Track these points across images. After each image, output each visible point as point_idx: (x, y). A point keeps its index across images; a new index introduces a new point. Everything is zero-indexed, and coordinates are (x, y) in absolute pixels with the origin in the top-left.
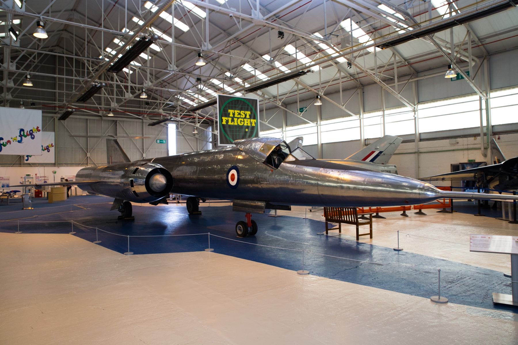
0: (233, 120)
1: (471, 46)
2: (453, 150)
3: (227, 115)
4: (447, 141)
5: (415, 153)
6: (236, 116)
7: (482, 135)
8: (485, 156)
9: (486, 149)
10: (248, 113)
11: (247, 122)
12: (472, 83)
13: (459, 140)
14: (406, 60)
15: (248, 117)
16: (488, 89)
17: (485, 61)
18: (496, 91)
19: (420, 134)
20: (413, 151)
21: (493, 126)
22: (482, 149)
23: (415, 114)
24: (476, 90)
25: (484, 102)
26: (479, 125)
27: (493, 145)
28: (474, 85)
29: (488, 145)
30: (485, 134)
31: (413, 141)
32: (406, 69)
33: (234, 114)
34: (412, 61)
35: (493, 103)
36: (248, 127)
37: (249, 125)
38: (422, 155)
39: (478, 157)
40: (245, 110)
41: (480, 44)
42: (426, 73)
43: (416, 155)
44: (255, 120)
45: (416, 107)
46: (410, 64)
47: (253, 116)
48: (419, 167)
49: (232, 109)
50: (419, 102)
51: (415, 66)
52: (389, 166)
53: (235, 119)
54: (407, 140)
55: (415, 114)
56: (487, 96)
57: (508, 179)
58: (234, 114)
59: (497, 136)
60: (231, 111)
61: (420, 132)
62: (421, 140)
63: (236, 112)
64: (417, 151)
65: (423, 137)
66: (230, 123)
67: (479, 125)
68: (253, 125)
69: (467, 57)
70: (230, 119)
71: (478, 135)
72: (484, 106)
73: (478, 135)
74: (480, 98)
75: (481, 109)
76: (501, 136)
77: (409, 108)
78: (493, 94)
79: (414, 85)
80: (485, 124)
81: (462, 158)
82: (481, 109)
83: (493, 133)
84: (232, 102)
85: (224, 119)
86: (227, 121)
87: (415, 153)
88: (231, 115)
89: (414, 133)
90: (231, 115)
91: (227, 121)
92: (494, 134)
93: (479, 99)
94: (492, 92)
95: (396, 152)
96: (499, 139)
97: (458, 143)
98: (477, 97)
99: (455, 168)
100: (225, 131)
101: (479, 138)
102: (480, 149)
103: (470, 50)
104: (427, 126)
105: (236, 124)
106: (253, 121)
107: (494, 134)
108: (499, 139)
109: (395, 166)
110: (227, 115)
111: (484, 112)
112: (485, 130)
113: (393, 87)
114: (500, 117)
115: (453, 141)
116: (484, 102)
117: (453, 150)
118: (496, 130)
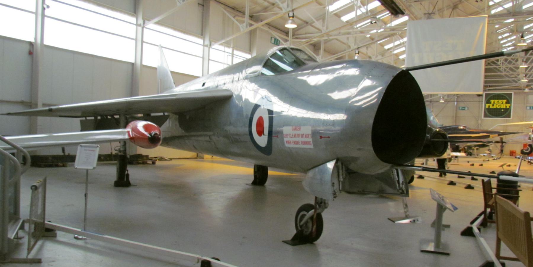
0: (493, 105)
3: (490, 103)
6: (496, 103)
10: (504, 101)
11: (503, 106)
15: (504, 103)
33: (494, 102)
36: (503, 109)
37: (504, 107)
40: (502, 99)
44: (509, 105)
47: (508, 102)
49: (493, 99)
53: (495, 105)
58: (494, 102)
60: (492, 101)
63: (496, 101)
66: (491, 107)
68: (508, 107)
70: (491, 105)
84: (494, 96)
85: (487, 105)
86: (489, 106)
88: (492, 103)
90: (492, 103)
91: (489, 106)
100: (488, 111)
105: (495, 107)
106: (508, 106)
110: (490, 103)
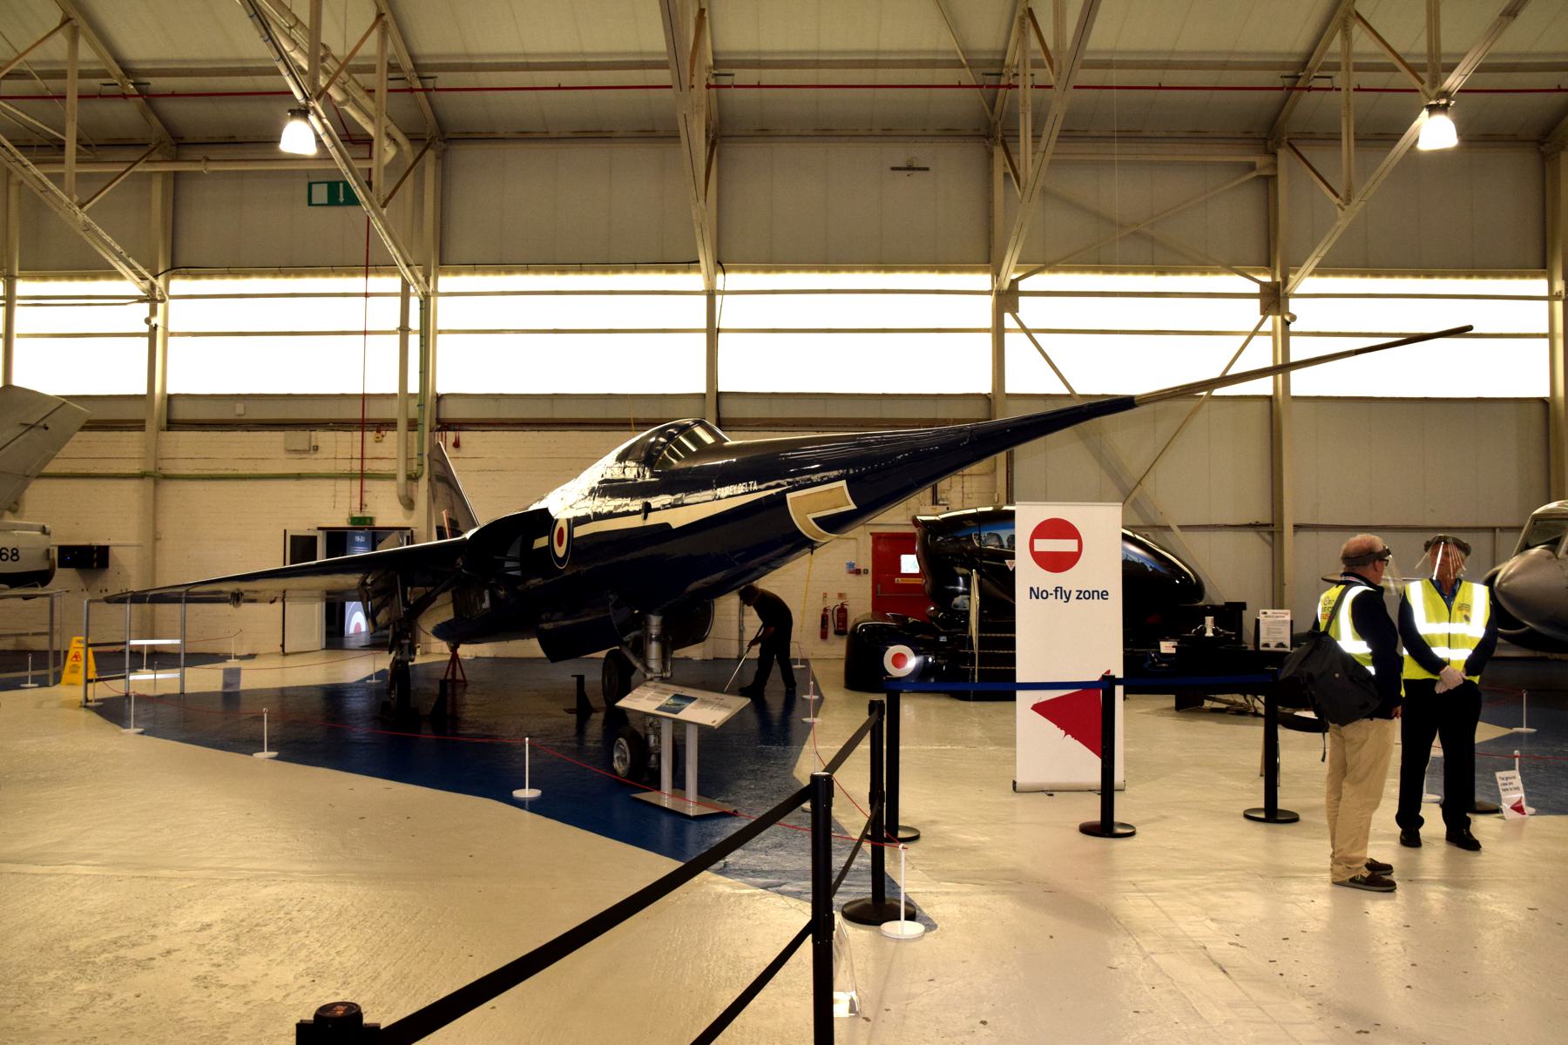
1: (386, 85)
2: (299, 477)
4: (278, 436)
5: (142, 476)
7: (402, 425)
8: (409, 504)
9: (413, 478)
12: (380, 216)
13: (323, 437)
14: (128, 72)
16: (433, 262)
17: (430, 154)
18: (457, 273)
19: (170, 398)
20: (135, 468)
21: (439, 398)
22: (401, 478)
23: (153, 312)
24: (393, 250)
25: (414, 303)
26: (396, 390)
27: (438, 468)
28: (386, 227)
29: (421, 465)
30: (413, 425)
31: (139, 425)
32: (124, 114)
34: (156, 83)
35: (447, 313)
38: (171, 488)
39: (386, 510)
41: (418, 85)
42: (214, 153)
43: (149, 483)
45: (160, 283)
46: (148, 97)
48: (156, 539)
50: (176, 268)
51: (172, 109)
52: (15, 527)
54: (106, 416)
55: (153, 312)
56: (427, 282)
57: (486, 605)
59: (451, 436)
61: (171, 390)
62: (172, 425)
64: (150, 468)
65: (181, 413)
67: (396, 390)
69: (371, 118)
71: (390, 425)
72: (414, 322)
73: (390, 425)
74: (406, 285)
75: (404, 330)
76: (465, 436)
77: (130, 286)
78: (446, 282)
79: (157, 189)
80: (414, 387)
81: (327, 508)
82: (404, 330)
83: (438, 421)
87: (142, 476)
89: (143, 390)
92: (445, 425)
93: (398, 289)
94: (445, 273)
95: (48, 469)
96: (457, 445)
97: (316, 448)
98: (392, 283)
99: (301, 547)
101: (391, 436)
102: (393, 477)
103: (381, 93)
104: (197, 372)
107: (445, 425)
108: (457, 445)
109: (44, 530)
111: (414, 341)
112: (414, 412)
113: (58, 179)
114: (464, 371)
115: (299, 438)
116: (414, 303)
117: (299, 477)
118: (451, 412)
